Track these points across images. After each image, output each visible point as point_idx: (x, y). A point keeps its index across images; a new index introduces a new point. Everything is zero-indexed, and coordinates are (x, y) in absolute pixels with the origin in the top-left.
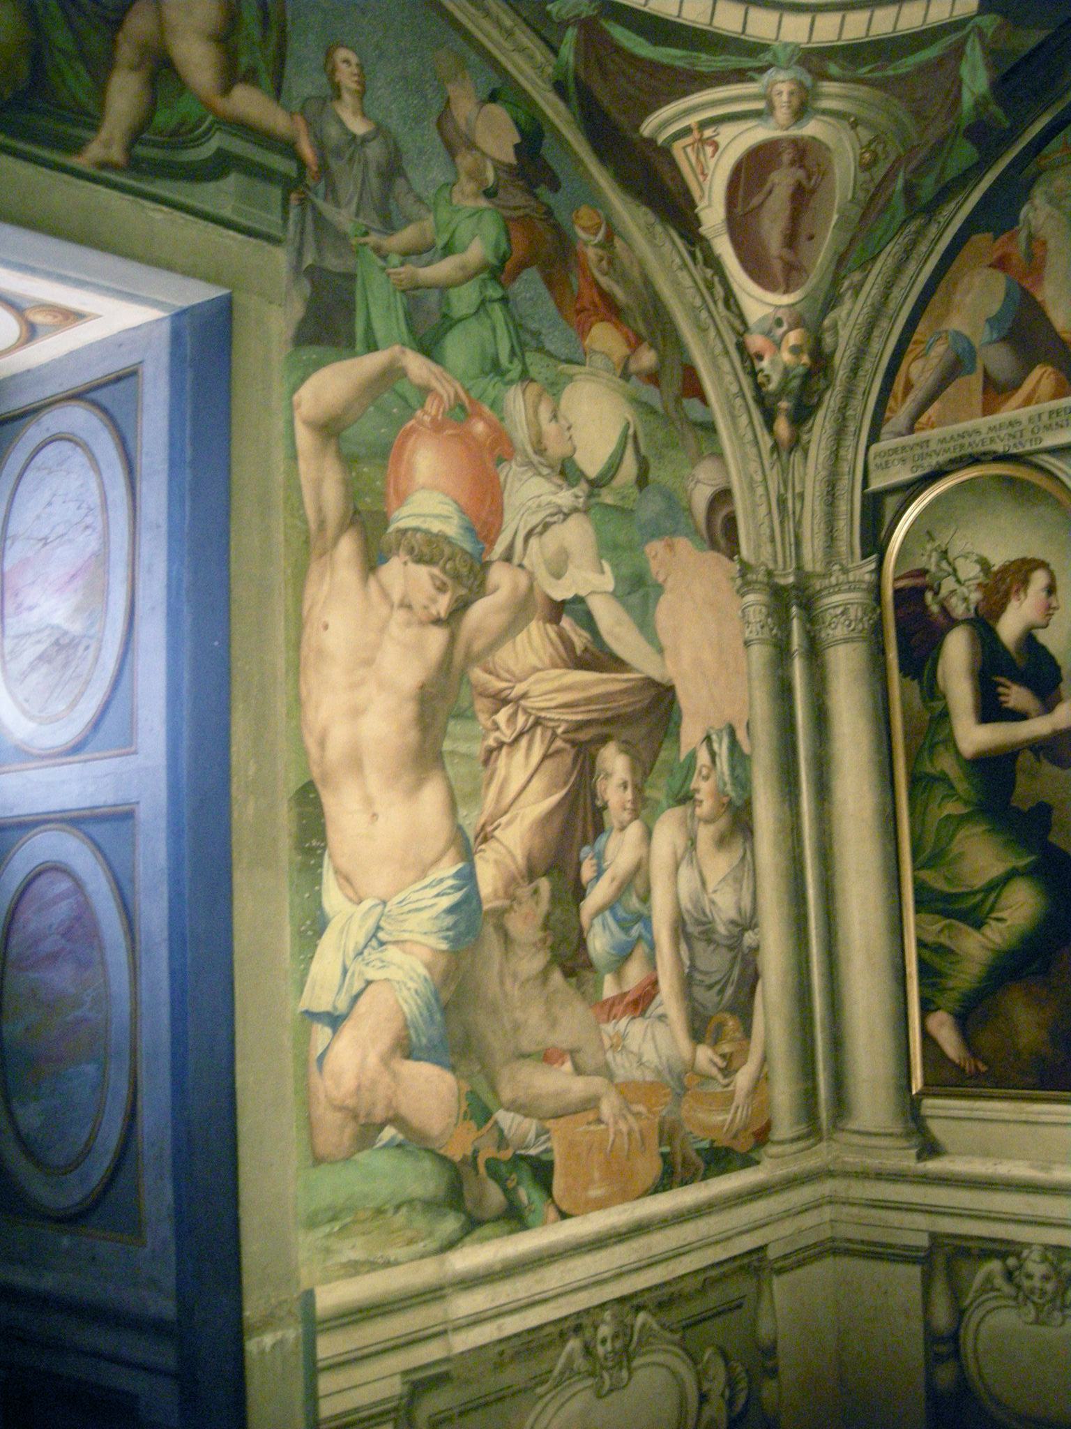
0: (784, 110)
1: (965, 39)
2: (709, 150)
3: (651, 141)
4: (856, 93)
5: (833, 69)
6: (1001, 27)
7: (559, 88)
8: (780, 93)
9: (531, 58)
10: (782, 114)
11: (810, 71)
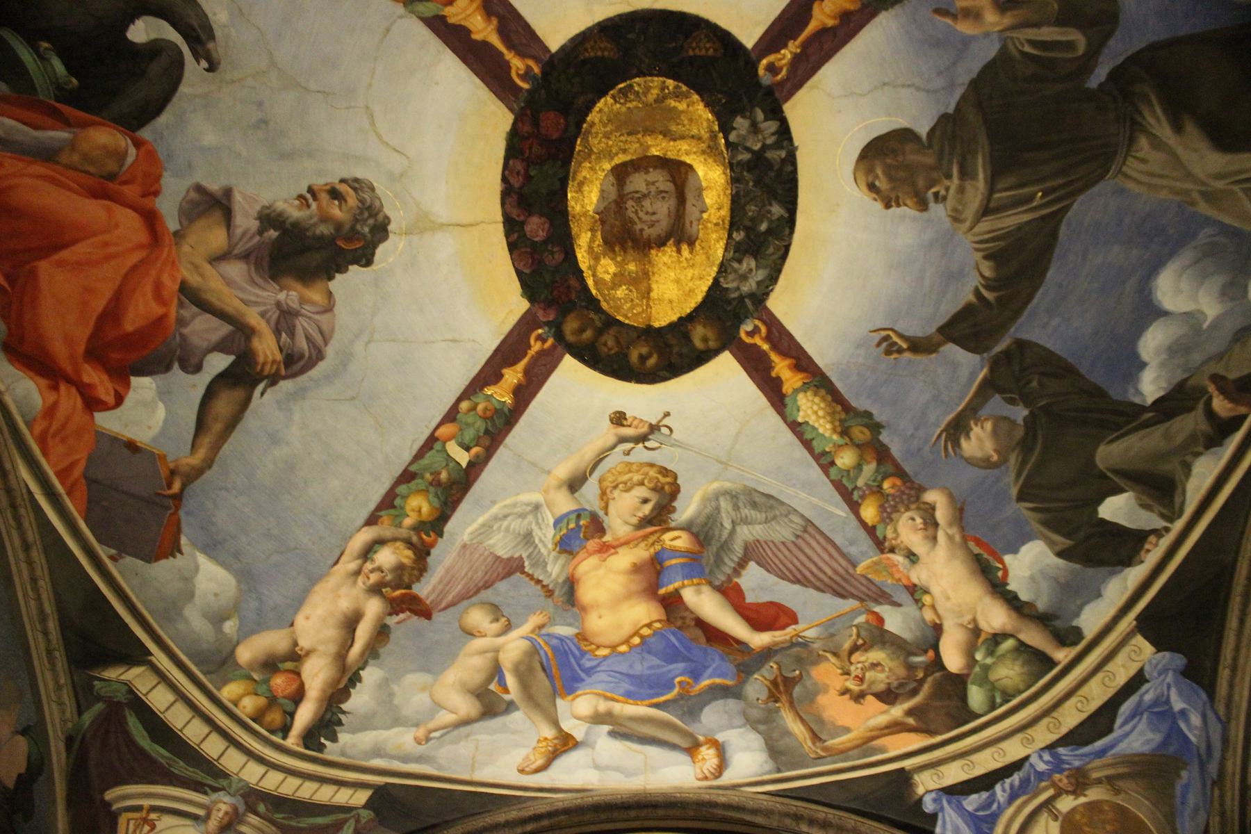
0: (215, 823)
1: (345, 821)
2: (147, 828)
3: (108, 805)
4: (266, 829)
5: (261, 808)
6: (371, 820)
7: (69, 741)
8: (219, 810)
9: (63, 712)
10: (213, 824)
11: (246, 803)
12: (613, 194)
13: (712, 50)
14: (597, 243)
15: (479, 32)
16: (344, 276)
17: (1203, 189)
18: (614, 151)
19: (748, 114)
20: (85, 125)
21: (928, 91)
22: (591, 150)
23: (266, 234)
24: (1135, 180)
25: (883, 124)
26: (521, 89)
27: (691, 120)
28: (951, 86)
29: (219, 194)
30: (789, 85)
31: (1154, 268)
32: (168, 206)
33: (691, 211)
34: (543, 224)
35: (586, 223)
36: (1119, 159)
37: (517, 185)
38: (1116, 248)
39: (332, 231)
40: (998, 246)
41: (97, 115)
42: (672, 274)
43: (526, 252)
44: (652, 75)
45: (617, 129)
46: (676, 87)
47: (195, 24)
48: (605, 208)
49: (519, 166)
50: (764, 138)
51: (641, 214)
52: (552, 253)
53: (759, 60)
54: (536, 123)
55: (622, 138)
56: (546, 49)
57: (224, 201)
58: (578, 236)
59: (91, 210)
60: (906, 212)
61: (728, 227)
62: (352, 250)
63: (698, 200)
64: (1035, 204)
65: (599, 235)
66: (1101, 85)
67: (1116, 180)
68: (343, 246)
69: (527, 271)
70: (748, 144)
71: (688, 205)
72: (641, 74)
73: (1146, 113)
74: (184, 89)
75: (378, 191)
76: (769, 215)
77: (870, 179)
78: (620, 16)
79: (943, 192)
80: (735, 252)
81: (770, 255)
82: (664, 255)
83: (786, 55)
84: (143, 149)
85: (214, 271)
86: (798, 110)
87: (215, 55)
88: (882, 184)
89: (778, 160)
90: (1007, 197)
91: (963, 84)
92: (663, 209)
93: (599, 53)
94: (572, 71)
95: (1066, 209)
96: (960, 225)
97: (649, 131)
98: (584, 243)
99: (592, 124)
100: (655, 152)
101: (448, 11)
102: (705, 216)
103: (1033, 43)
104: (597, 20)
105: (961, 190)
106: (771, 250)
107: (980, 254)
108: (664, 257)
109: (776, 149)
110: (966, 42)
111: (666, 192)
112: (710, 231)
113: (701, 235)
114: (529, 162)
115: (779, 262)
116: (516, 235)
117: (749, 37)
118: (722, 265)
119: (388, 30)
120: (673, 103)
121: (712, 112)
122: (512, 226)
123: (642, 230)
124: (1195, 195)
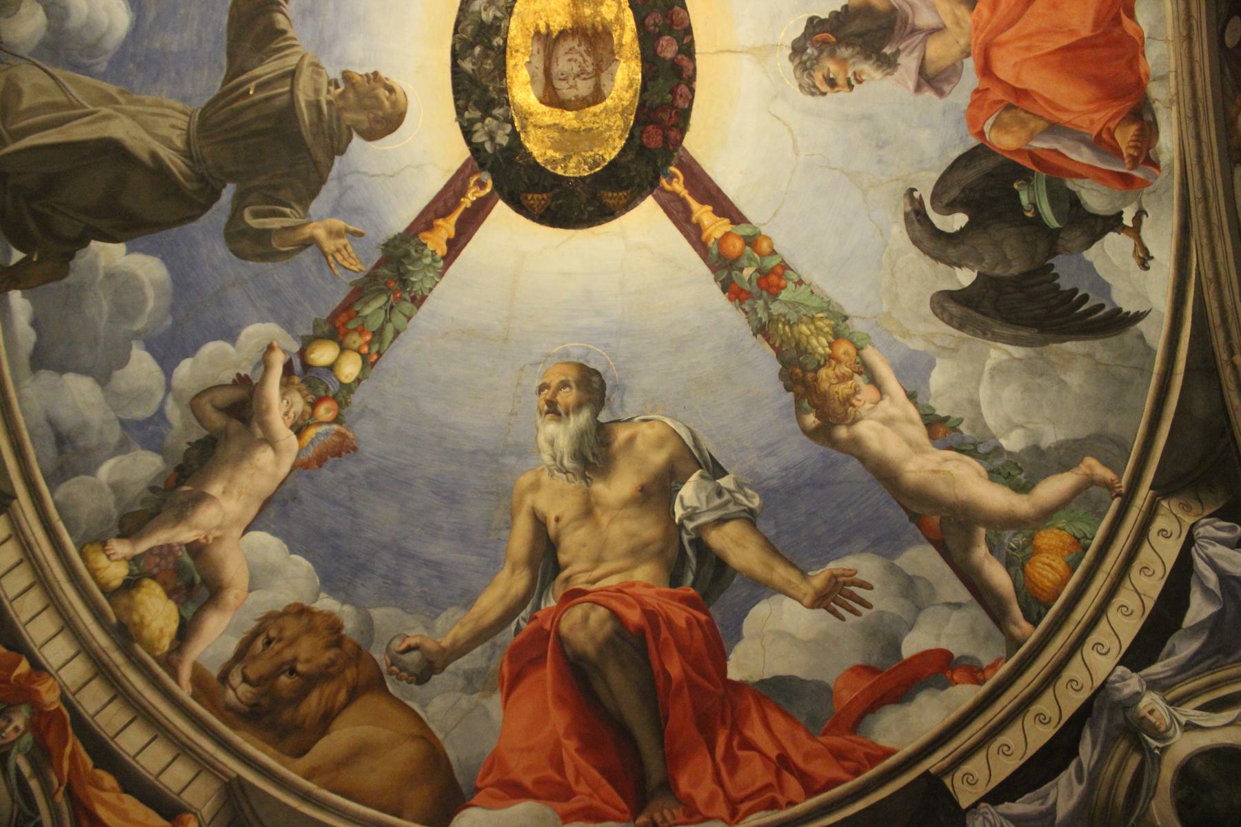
12: (604, 77)
13: (529, 198)
14: (617, 34)
15: (706, 211)
16: (835, 9)
17: (118, 106)
18: (603, 115)
19: (498, 148)
20: (1019, 152)
21: (358, 172)
22: (622, 115)
23: (894, 50)
24: (174, 109)
25: (388, 143)
26: (677, 166)
27: (543, 142)
28: (340, 178)
29: (926, 88)
30: (468, 171)
31: (136, 30)
32: (970, 79)
33: (539, 64)
34: (661, 53)
35: (627, 52)
36: (194, 127)
37: (683, 86)
38: (175, 48)
39: (838, 51)
40: (277, 44)
41: (1007, 159)
42: (553, 5)
43: (677, 26)
44: (575, 178)
45: (601, 133)
46: (555, 168)
47: (917, 225)
48: (611, 65)
49: (681, 103)
50: (483, 128)
51: (580, 59)
52: (655, 25)
53: (492, 192)
54: (666, 138)
55: (597, 126)
56: (656, 198)
57: (923, 81)
58: (633, 40)
59: (1033, 80)
60: (360, 70)
61: (508, 49)
62: (824, 32)
63: (534, 72)
64: (253, 84)
65: (616, 42)
66: (224, 186)
67: (191, 109)
68: (831, 36)
69: (677, 8)
70: (495, 122)
71: (541, 67)
72: (583, 179)
73: (183, 167)
74: (936, 176)
75: (797, 84)
76: (474, 60)
77: (393, 96)
78: (600, 224)
79: (332, 89)
80: (500, 26)
81: (469, 25)
82: (560, 22)
83: (471, 196)
84: (978, 129)
85: (944, 19)
86: (460, 153)
87: (907, 201)
88: (383, 93)
89: (470, 110)
90: (275, 88)
91: (332, 179)
92: (563, 64)
93: (615, 195)
94: (637, 181)
95: (227, 80)
96: (311, 60)
97: (576, 132)
98: (627, 34)
99: (621, 137)
100: (570, 114)
101: (729, 228)
102: (527, 59)
103: (284, 215)
104: (617, 220)
105: (317, 91)
106: (469, 29)
107: (289, 35)
108: (560, 20)
109: (473, 119)
110: (335, 213)
111: (560, 79)
112: (523, 45)
113: (530, 41)
114: (672, 106)
115: (462, 18)
116: (685, 41)
117: (501, 209)
118: (510, 16)
119: (775, 214)
120: (558, 155)
121: (526, 149)
122: (688, 50)
123: (580, 45)
124: (121, 99)
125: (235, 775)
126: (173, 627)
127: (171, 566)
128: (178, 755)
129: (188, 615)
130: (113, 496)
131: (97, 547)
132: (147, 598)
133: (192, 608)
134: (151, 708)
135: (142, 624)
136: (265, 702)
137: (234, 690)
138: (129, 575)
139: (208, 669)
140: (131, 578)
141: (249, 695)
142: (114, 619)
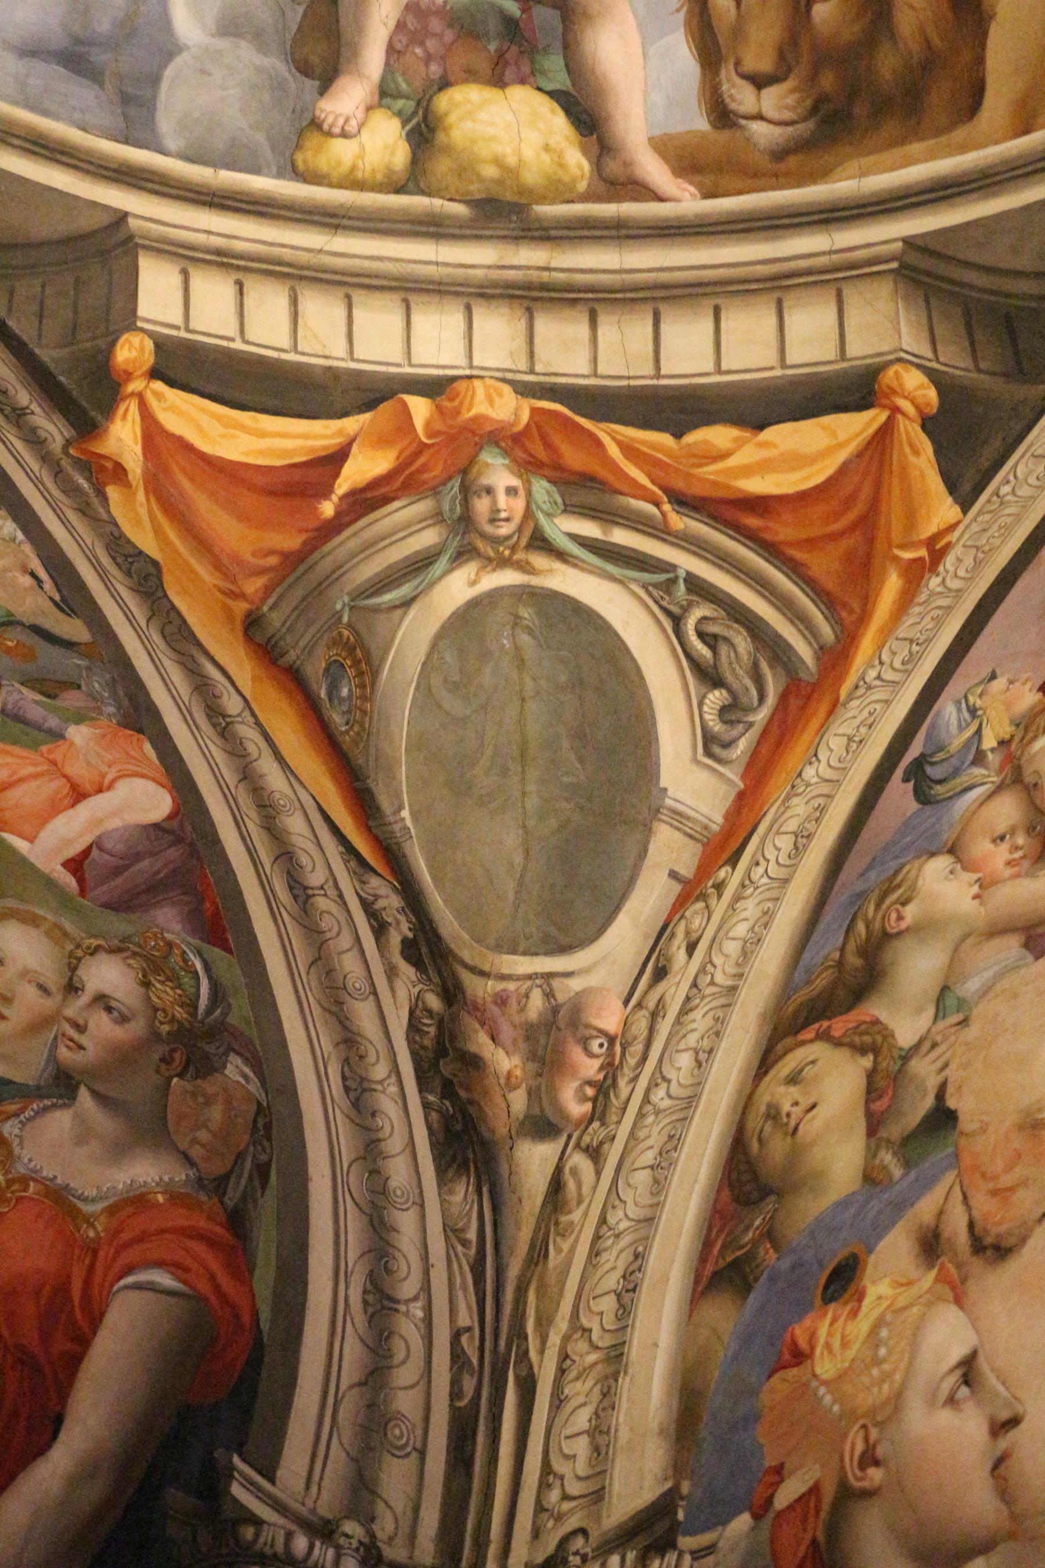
125: (900, 244)
126: (559, 123)
127: (449, 36)
128: (780, 302)
129: (560, 80)
130: (243, 43)
131: (313, 140)
132: (469, 125)
133: (554, 63)
134: (664, 277)
135: (509, 173)
136: (828, 81)
137: (760, 117)
138: (404, 124)
139: (681, 128)
140: (414, 122)
141: (790, 100)
142: (460, 209)
